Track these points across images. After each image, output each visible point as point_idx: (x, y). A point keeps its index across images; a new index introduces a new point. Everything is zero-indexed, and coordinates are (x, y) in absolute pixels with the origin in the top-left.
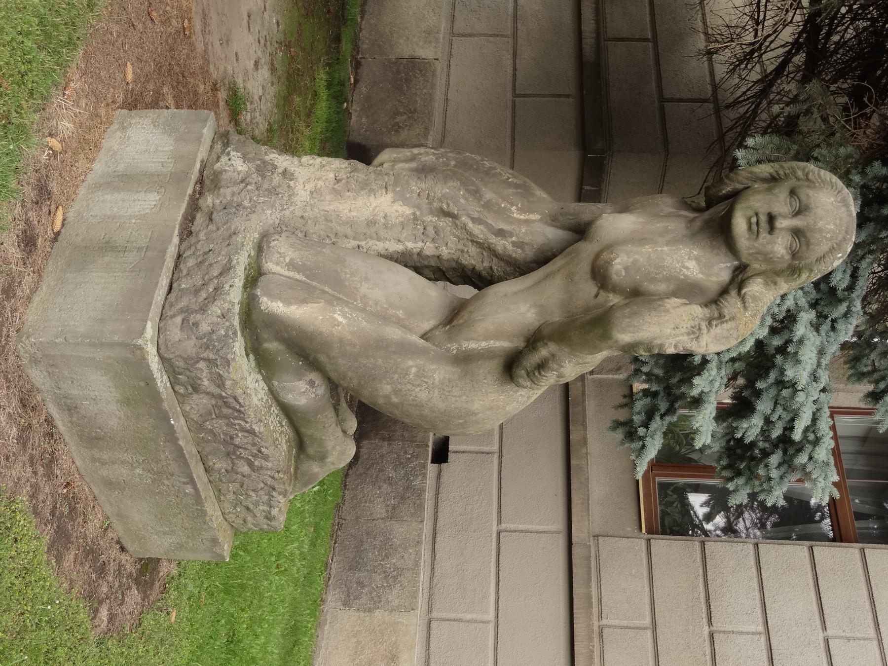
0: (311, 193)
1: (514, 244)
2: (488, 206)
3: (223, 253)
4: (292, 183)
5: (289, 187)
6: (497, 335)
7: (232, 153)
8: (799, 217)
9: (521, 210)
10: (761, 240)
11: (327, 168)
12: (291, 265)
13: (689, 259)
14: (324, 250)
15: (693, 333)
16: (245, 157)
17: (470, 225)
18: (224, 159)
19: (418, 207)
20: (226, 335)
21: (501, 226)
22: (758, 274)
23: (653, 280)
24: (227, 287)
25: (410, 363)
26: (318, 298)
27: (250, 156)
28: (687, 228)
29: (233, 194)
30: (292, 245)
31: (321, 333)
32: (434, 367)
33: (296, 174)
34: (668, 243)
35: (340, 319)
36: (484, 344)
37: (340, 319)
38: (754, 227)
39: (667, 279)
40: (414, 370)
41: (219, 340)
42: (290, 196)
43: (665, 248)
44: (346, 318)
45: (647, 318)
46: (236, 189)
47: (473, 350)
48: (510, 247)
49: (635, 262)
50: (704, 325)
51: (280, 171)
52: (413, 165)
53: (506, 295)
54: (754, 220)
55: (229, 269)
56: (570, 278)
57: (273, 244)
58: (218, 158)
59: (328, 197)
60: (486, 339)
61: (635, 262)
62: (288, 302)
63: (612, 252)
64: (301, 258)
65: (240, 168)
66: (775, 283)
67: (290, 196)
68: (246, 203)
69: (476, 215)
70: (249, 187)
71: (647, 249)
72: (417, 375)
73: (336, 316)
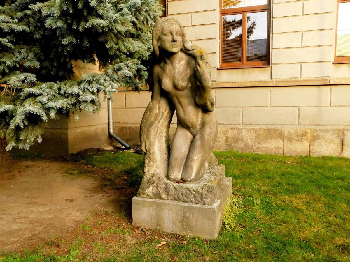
0: (157, 168)
1: (165, 112)
2: (156, 119)
4: (155, 174)
5: (157, 175)
7: (147, 191)
8: (173, 33)
9: (156, 110)
10: (178, 44)
11: (149, 165)
12: (179, 172)
13: (179, 64)
15: (206, 64)
16: (148, 187)
17: (160, 124)
18: (148, 193)
19: (156, 138)
20: (207, 187)
21: (161, 116)
22: (184, 45)
23: (186, 74)
25: (206, 138)
29: (161, 190)
31: (200, 162)
32: (206, 132)
34: (174, 69)
35: (196, 157)
38: (176, 46)
39: (186, 70)
40: (208, 137)
41: (209, 188)
42: (159, 174)
43: (176, 70)
44: (196, 156)
45: (206, 76)
46: (159, 189)
47: (201, 122)
48: (166, 113)
49: (181, 79)
50: (204, 61)
51: (151, 178)
52: (147, 141)
54: (174, 46)
55: (187, 188)
56: (182, 96)
57: (173, 177)
58: (148, 195)
59: (157, 163)
60: (198, 118)
61: (181, 79)
62: (192, 172)
64: (177, 169)
65: (152, 189)
66: (186, 40)
67: (159, 174)
68: (164, 186)
69: (158, 122)
70: (159, 186)
72: (209, 136)
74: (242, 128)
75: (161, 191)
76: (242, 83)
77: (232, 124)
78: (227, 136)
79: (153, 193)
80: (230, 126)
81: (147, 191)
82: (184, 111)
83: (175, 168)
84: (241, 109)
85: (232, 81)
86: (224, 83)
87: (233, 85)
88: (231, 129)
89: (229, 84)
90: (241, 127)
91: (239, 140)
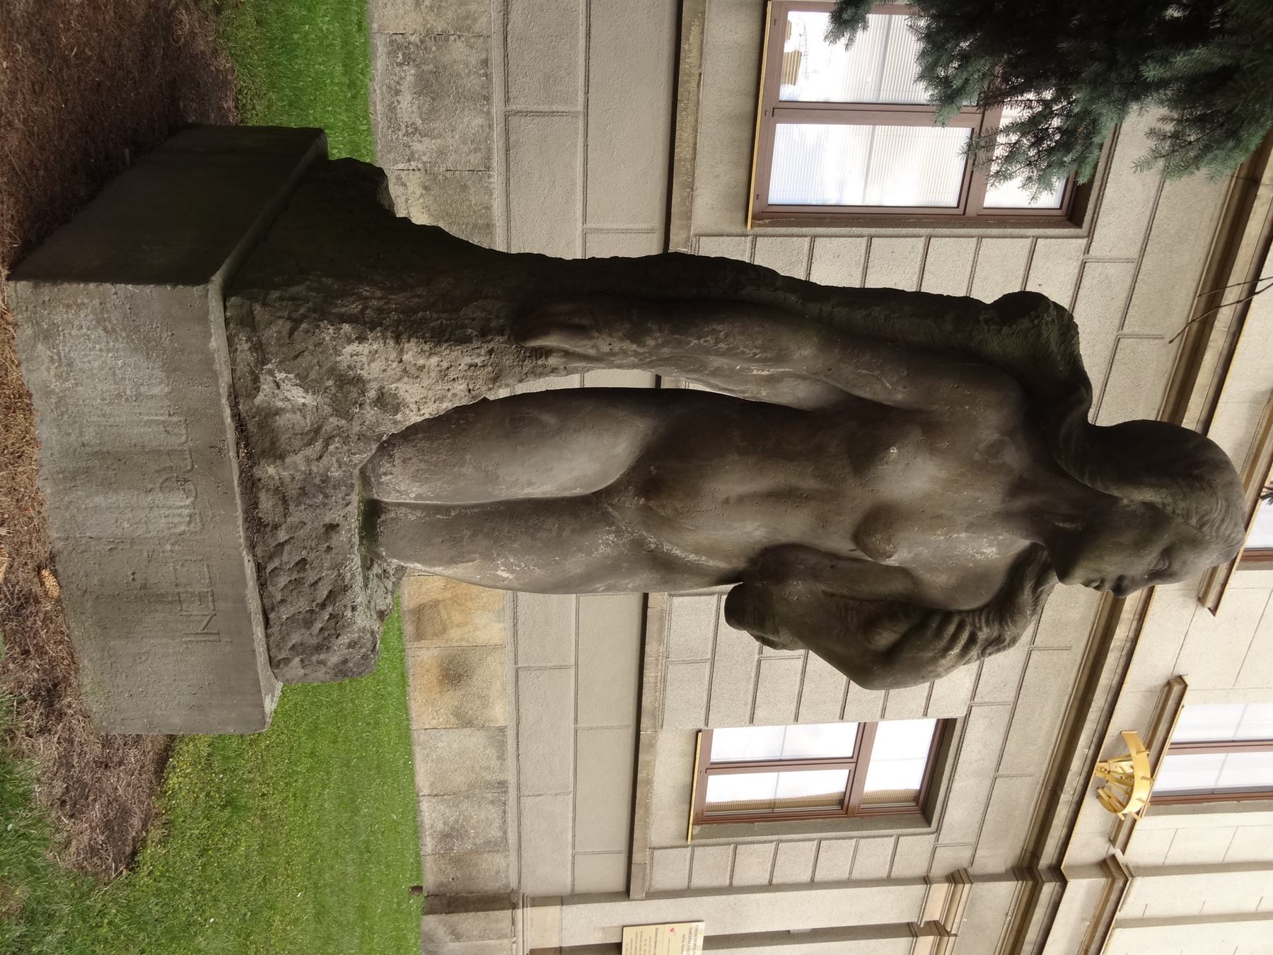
3: (327, 564)
6: (711, 552)
14: (464, 470)
16: (304, 381)
18: (266, 386)
24: (349, 614)
26: (469, 553)
27: (313, 375)
28: (1004, 501)
29: (308, 460)
30: (415, 478)
33: (401, 393)
34: (970, 527)
35: (505, 575)
36: (692, 557)
37: (505, 575)
43: (963, 535)
44: (512, 572)
46: (310, 452)
51: (372, 394)
53: (727, 501)
58: (256, 380)
60: (697, 552)
63: (889, 541)
71: (939, 537)
73: (499, 573)
74: (488, 113)
75: (299, 459)
76: (691, 118)
77: (506, 64)
78: (447, 40)
79: (278, 412)
80: (496, 56)
81: (280, 376)
82: (741, 499)
83: (439, 484)
84: (580, 108)
85: (708, 67)
86: (702, 32)
87: (690, 75)
88: (485, 62)
89: (695, 53)
90: (497, 108)
91: (433, 99)
